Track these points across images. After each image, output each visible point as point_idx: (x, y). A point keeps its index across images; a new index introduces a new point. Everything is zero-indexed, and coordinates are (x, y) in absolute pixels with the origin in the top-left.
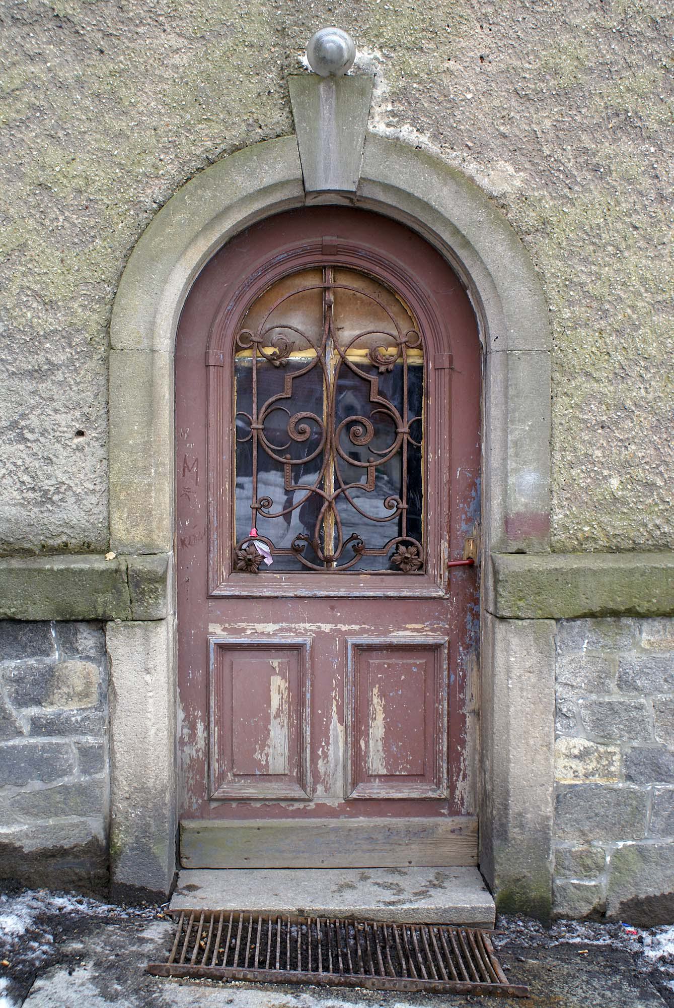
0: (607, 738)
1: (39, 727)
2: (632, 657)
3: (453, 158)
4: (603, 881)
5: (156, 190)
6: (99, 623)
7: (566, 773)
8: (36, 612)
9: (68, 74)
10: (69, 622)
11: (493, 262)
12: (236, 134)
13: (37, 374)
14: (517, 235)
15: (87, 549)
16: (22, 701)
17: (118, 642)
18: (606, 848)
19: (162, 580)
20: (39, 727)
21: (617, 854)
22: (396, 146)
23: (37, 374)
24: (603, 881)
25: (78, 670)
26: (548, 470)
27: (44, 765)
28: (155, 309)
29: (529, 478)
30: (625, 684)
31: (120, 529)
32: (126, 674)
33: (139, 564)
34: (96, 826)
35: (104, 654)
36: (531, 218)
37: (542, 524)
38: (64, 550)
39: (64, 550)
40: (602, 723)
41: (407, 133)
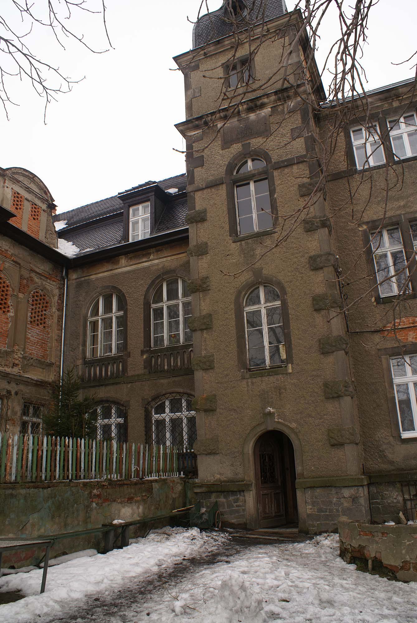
0: (314, 506)
1: (237, 506)
2: (316, 494)
3: (286, 423)
4: (316, 528)
5: (248, 431)
6: (243, 491)
7: (309, 512)
8: (235, 490)
9: (236, 417)
10: (240, 491)
11: (292, 437)
12: (257, 423)
13: (235, 457)
14: (296, 434)
15: (242, 481)
16: (234, 503)
17: (246, 494)
18: (316, 523)
19: (251, 485)
20: (237, 506)
21: (317, 524)
22: (278, 422)
23: (235, 457)
24: (316, 528)
25: (241, 498)
26: (303, 466)
27: (237, 511)
28: (250, 448)
29: (300, 468)
30: (316, 498)
31: (246, 478)
32: (247, 498)
33: (248, 483)
34: (245, 520)
35: (244, 496)
36: (298, 431)
37: (303, 474)
38: (239, 481)
39: (239, 481)
40: (313, 504)
41: (280, 420)
